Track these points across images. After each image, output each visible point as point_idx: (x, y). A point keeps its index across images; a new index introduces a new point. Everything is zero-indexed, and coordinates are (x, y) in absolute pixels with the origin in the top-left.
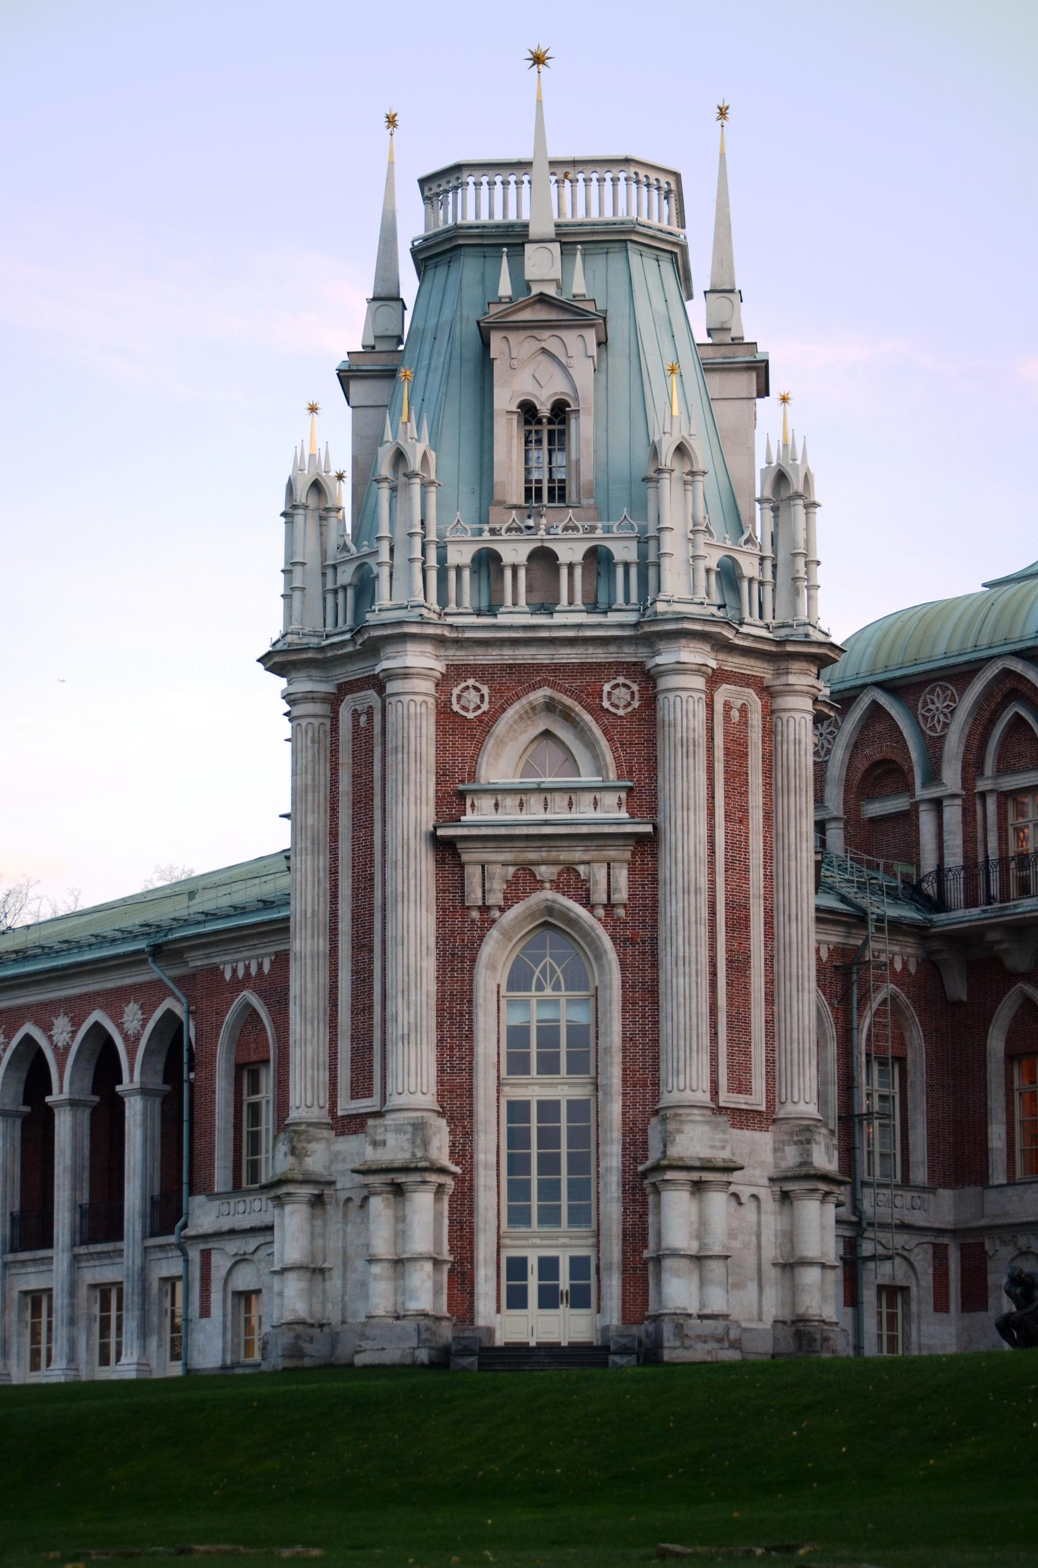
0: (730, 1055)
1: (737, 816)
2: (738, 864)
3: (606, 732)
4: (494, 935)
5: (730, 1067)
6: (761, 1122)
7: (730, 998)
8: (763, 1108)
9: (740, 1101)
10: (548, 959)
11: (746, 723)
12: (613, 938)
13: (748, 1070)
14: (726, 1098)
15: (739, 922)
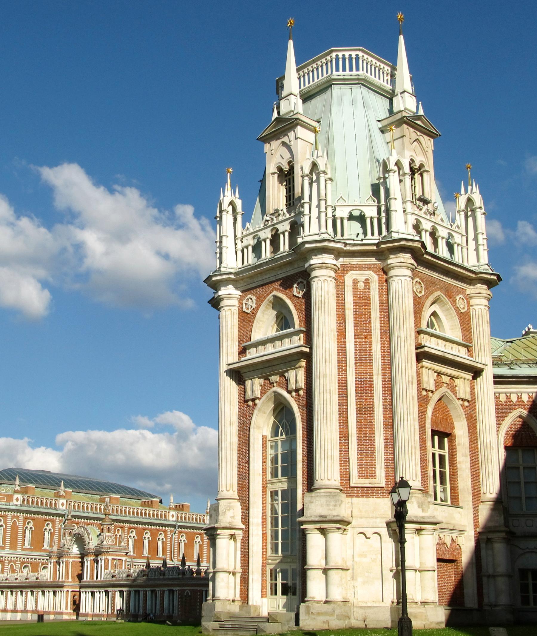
0: (360, 459)
1: (363, 334)
2: (363, 358)
3: (295, 306)
4: (256, 412)
5: (360, 465)
6: (383, 493)
7: (359, 429)
8: (383, 485)
9: (366, 482)
10: (284, 420)
11: (369, 288)
12: (299, 406)
13: (373, 465)
14: (355, 481)
15: (365, 387)
